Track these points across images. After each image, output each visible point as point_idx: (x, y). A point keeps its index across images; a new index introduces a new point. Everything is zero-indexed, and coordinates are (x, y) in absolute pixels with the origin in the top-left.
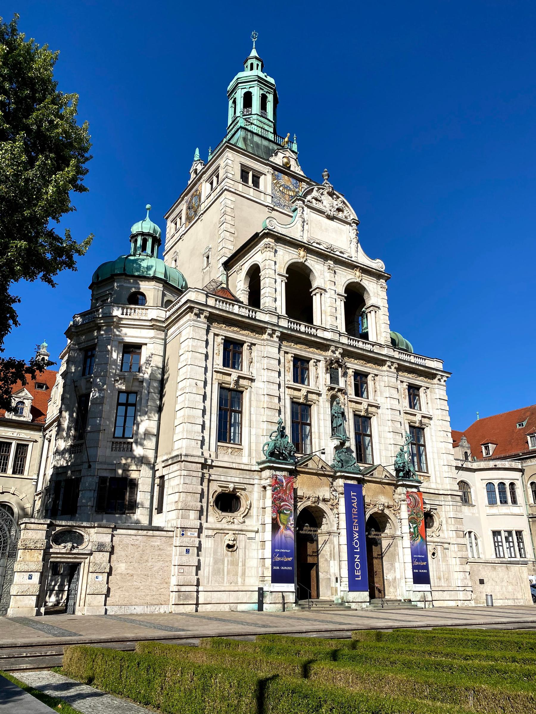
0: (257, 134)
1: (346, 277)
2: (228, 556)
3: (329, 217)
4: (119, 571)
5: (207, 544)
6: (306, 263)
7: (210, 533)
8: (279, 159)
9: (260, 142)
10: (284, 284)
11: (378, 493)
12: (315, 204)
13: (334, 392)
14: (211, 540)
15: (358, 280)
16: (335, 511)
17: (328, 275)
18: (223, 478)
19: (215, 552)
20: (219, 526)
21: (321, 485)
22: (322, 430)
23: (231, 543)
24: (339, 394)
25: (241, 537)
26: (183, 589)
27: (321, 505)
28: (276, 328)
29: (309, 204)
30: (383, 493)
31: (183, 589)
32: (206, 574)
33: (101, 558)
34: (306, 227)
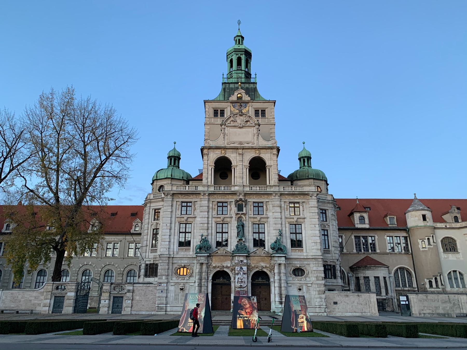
0: (231, 83)
1: (250, 155)
2: (181, 293)
3: (240, 128)
4: (136, 299)
5: (172, 288)
6: (226, 156)
7: (173, 284)
8: (234, 98)
9: (233, 87)
10: (213, 170)
11: (260, 262)
12: (232, 124)
13: (239, 216)
14: (173, 287)
15: (257, 155)
16: (233, 272)
17: (239, 158)
18: (179, 262)
19: (175, 292)
20: (176, 281)
21: (226, 260)
22: (232, 235)
23: (181, 288)
24: (242, 216)
25: (187, 285)
26: (160, 306)
27: (225, 270)
28: (206, 192)
29: (229, 125)
30: (263, 261)
31: (160, 306)
32: (171, 300)
33: (129, 295)
34: (226, 137)
